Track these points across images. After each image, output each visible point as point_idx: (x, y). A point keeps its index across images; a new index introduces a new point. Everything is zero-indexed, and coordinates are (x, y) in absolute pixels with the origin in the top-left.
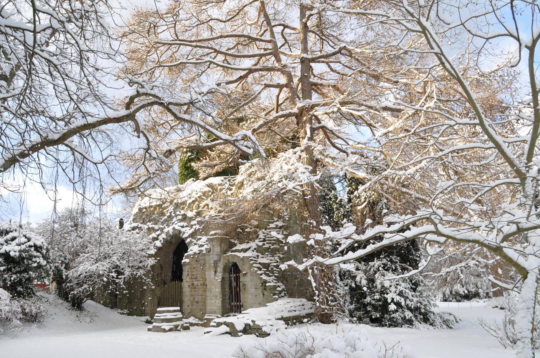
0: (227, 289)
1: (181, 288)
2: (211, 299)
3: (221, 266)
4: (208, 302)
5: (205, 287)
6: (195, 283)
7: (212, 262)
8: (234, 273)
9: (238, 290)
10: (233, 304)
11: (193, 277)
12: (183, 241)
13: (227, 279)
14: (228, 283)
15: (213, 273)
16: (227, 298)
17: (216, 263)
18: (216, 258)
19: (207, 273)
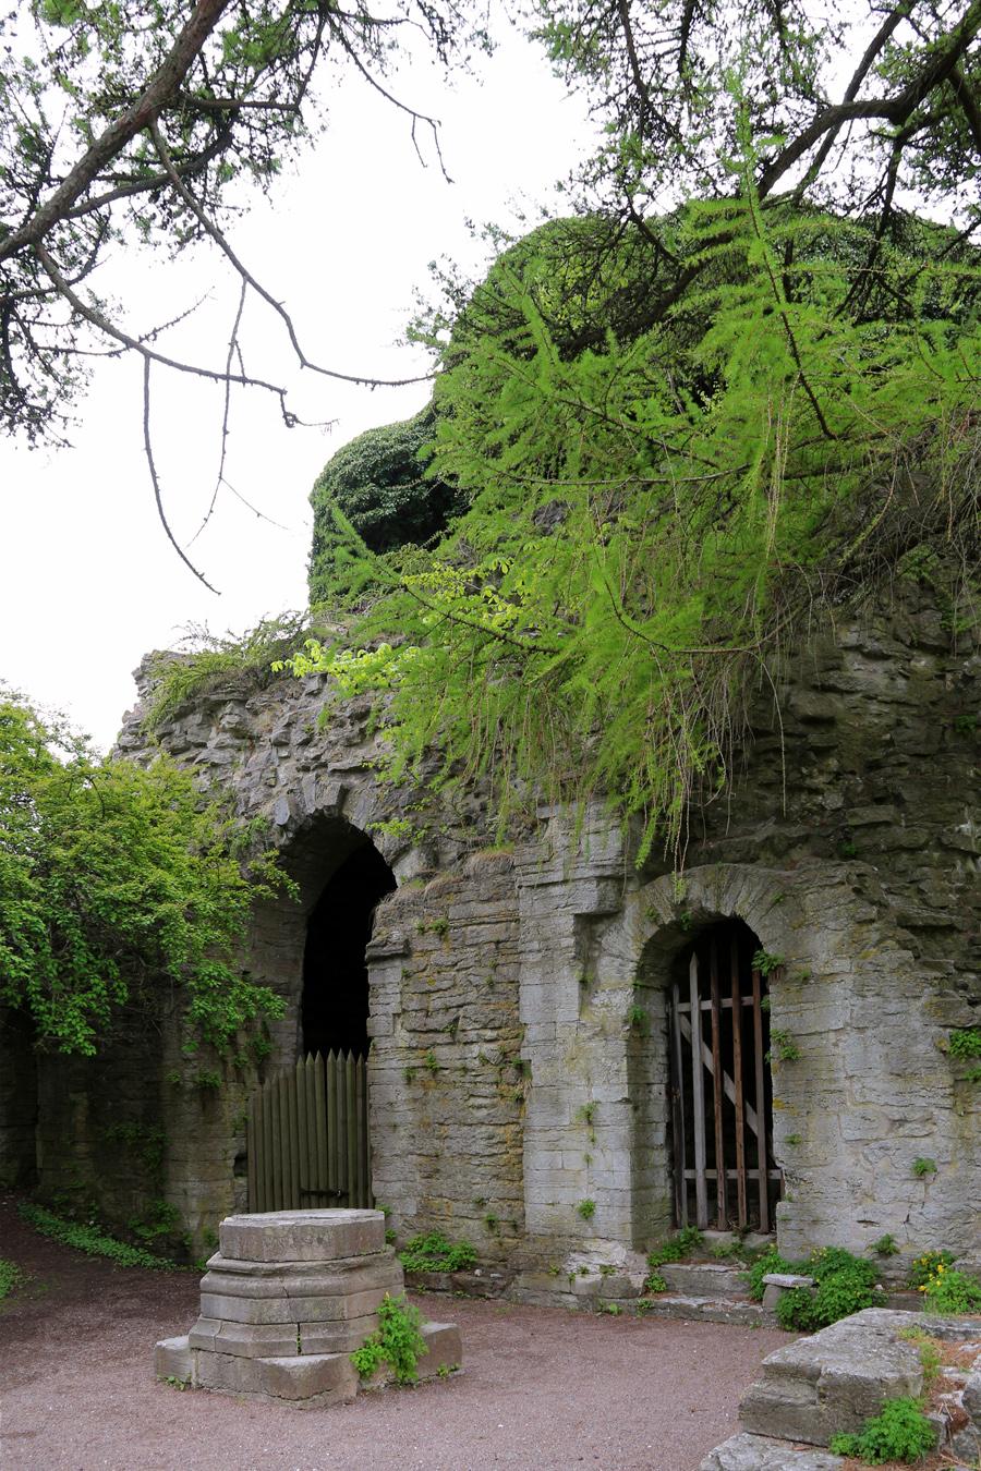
0: (658, 1090)
1: (361, 1089)
2: (553, 1146)
3: (624, 946)
4: (538, 1160)
5: (510, 1073)
6: (446, 1054)
7: (567, 924)
8: (704, 995)
9: (734, 1092)
10: (687, 1174)
11: (433, 1023)
12: (363, 843)
13: (656, 1029)
14: (662, 1050)
15: (569, 986)
16: (659, 1137)
17: (591, 924)
18: (588, 899)
19: (531, 996)
